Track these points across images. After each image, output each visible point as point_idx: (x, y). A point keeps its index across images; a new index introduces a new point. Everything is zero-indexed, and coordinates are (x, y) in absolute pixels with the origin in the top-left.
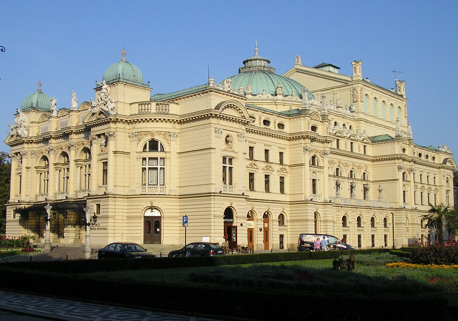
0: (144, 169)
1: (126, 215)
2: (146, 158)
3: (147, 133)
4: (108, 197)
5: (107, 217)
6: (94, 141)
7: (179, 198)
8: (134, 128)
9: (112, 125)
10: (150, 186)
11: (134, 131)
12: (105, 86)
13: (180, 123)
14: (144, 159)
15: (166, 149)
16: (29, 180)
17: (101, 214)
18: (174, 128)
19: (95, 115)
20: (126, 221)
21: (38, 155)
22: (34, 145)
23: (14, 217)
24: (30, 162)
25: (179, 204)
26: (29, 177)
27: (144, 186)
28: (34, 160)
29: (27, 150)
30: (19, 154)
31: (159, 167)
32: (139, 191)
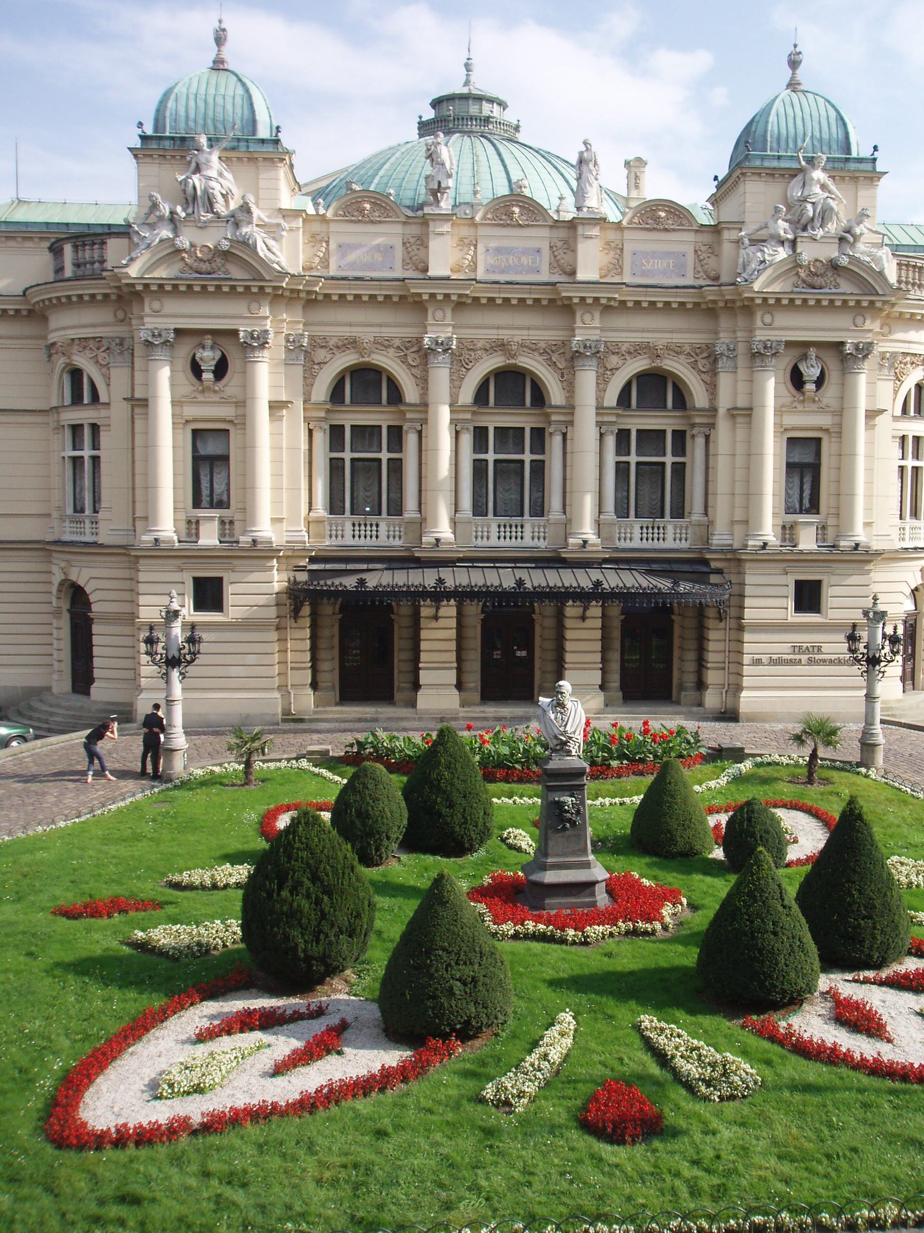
12: (818, 175)
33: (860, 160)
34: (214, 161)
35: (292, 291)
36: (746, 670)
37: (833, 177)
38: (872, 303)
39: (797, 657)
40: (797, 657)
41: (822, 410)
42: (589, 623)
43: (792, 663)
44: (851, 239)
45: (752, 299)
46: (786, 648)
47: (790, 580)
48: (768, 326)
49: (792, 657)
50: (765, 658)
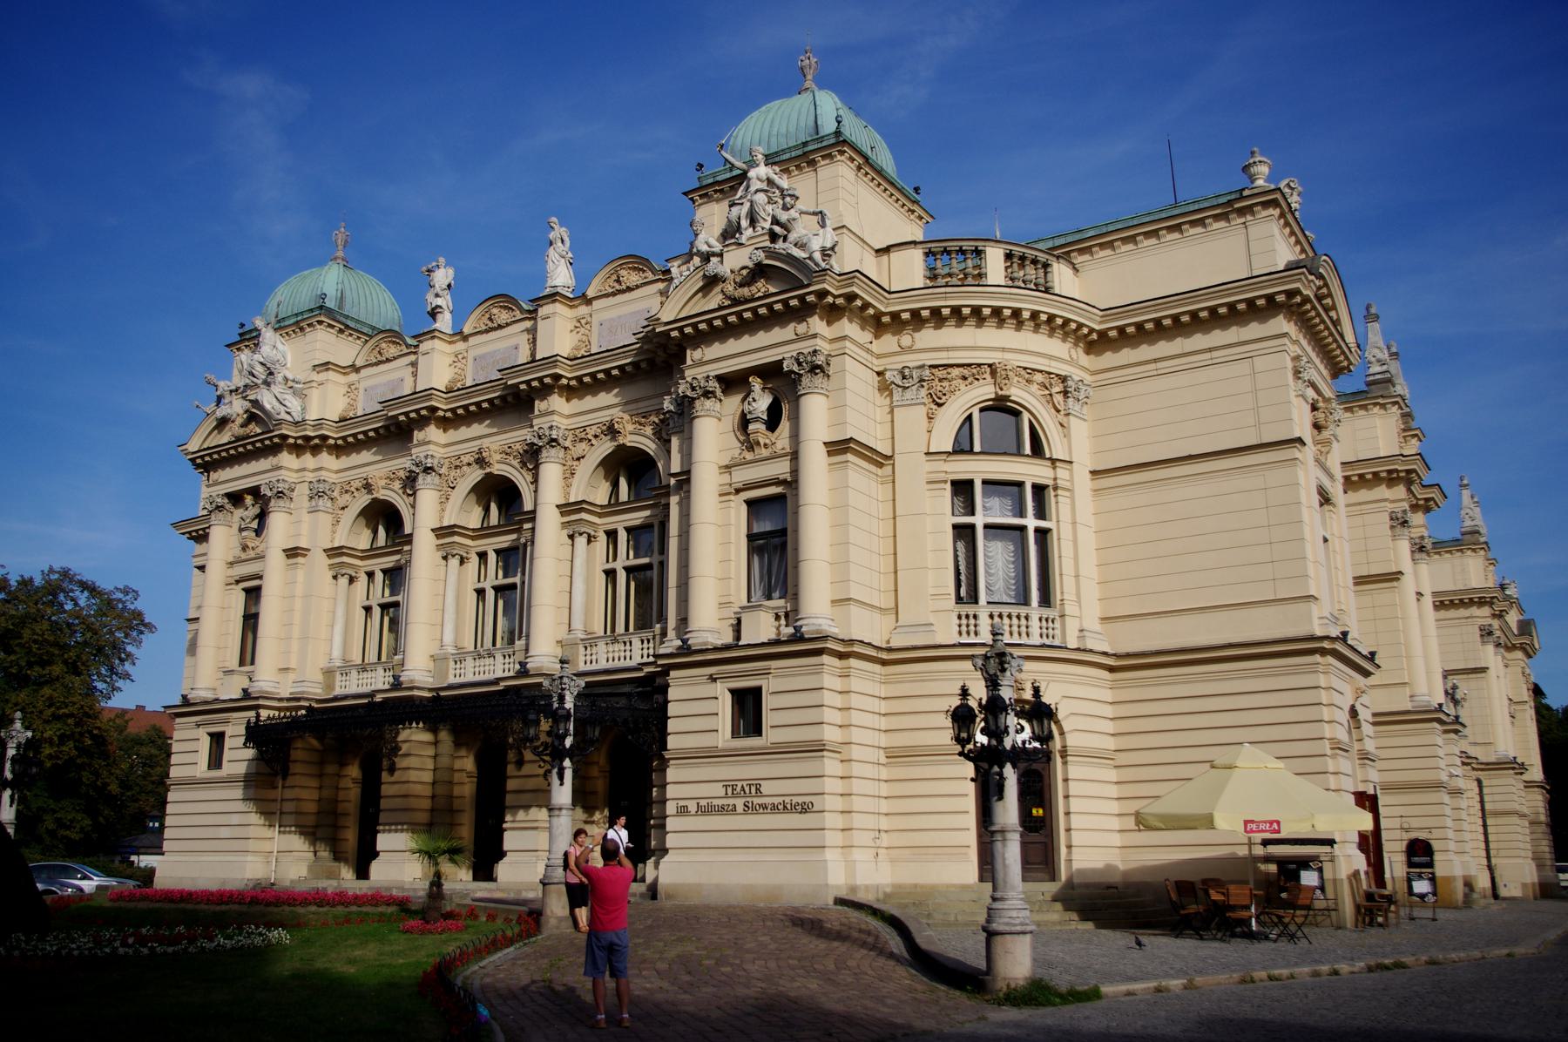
0: (964, 533)
1: (884, 740)
2: (970, 483)
3: (971, 371)
4: (819, 652)
5: (816, 749)
6: (704, 405)
7: (1112, 669)
8: (904, 350)
9: (816, 324)
10: (996, 610)
11: (912, 360)
12: (762, 171)
13: (1097, 343)
14: (963, 489)
15: (1055, 445)
16: (298, 604)
17: (770, 736)
18: (1071, 362)
19: (718, 289)
20: (884, 773)
21: (341, 501)
22: (326, 459)
23: (216, 761)
24: (305, 528)
25: (1108, 695)
26: (299, 590)
27: (970, 610)
28: (325, 520)
29: (291, 477)
30: (249, 500)
31: (1031, 523)
32: (947, 631)
33: (821, 139)
34: (268, 336)
35: (307, 439)
36: (671, 824)
37: (786, 171)
38: (802, 298)
39: (731, 801)
40: (731, 801)
41: (775, 457)
42: (526, 769)
43: (722, 810)
44: (777, 229)
45: (666, 334)
46: (718, 790)
47: (722, 691)
48: (702, 363)
49: (725, 801)
50: (692, 807)
